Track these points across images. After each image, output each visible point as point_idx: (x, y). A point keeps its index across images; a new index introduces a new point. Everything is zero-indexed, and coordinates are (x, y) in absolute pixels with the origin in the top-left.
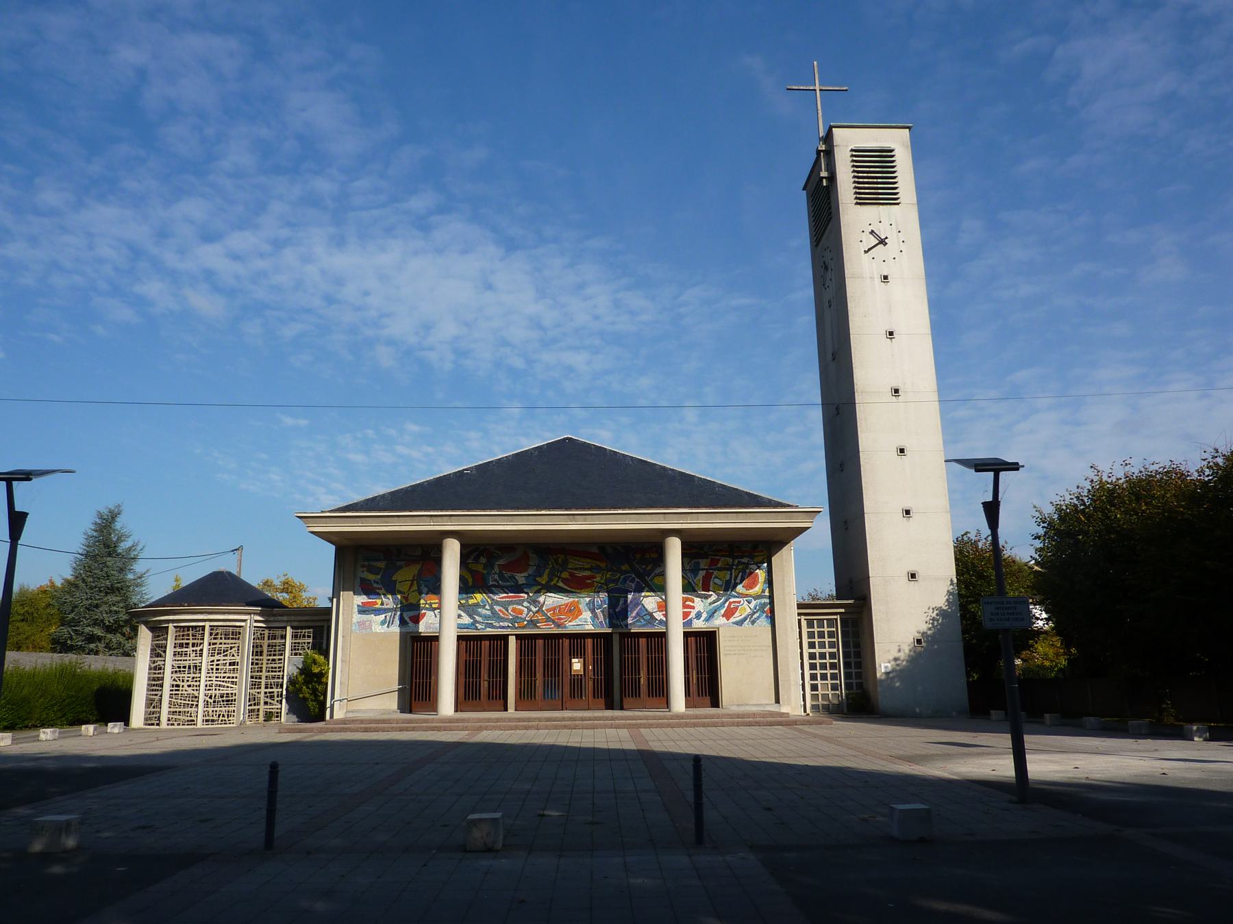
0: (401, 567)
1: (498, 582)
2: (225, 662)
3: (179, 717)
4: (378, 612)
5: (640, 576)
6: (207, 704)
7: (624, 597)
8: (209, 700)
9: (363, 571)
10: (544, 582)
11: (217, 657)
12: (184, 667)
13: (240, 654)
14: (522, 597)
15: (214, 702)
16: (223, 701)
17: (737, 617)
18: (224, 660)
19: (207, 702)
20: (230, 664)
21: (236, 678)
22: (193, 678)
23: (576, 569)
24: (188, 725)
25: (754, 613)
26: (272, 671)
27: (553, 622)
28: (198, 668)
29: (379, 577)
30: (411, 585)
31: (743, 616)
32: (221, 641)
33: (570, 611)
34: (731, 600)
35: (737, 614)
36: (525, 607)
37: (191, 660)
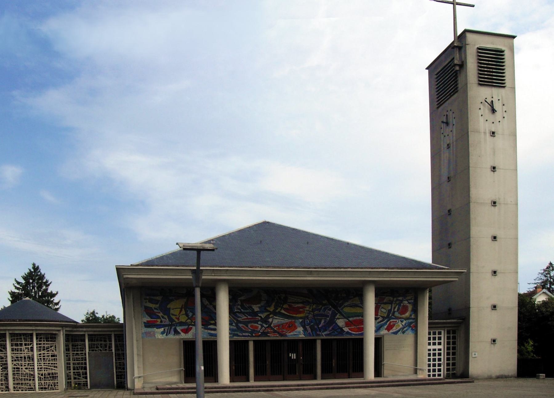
0: (172, 300)
1: (240, 310)
2: (48, 355)
3: (22, 386)
4: (159, 327)
5: (335, 307)
6: (40, 379)
7: (324, 319)
8: (41, 377)
9: (146, 302)
10: (271, 310)
11: (42, 352)
12: (21, 358)
13: (57, 350)
14: (257, 319)
15: (45, 378)
16: (50, 377)
17: (394, 329)
18: (47, 354)
19: (40, 377)
20: (52, 356)
21: (56, 364)
22: (29, 364)
23: (293, 303)
24: (29, 391)
25: (405, 327)
26: (77, 360)
27: (278, 333)
28: (31, 358)
29: (158, 305)
30: (181, 311)
31: (398, 329)
32: (44, 342)
33: (289, 327)
34: (391, 321)
35: (394, 328)
36: (260, 325)
37: (26, 353)
